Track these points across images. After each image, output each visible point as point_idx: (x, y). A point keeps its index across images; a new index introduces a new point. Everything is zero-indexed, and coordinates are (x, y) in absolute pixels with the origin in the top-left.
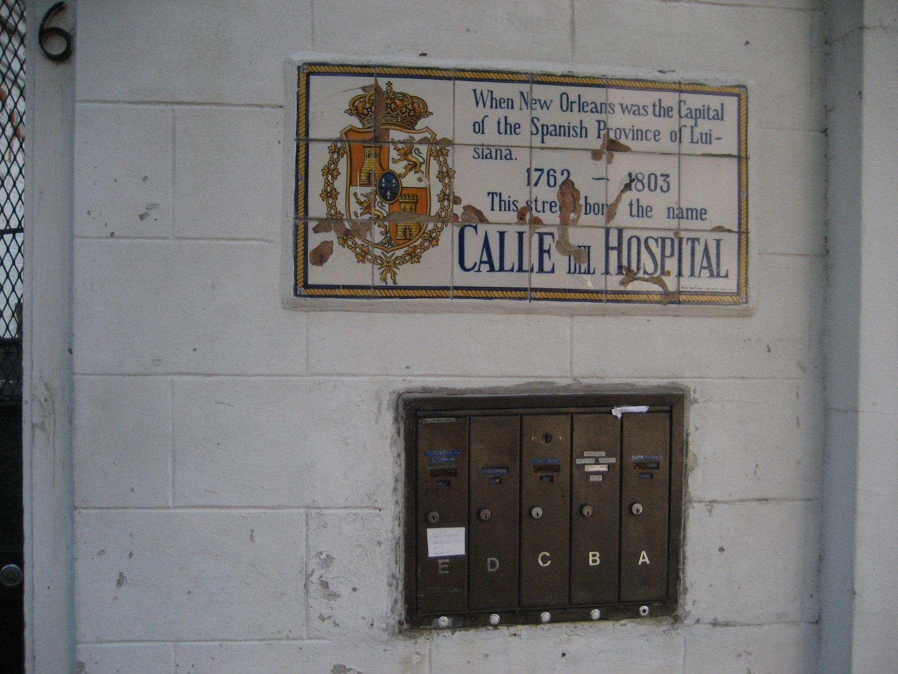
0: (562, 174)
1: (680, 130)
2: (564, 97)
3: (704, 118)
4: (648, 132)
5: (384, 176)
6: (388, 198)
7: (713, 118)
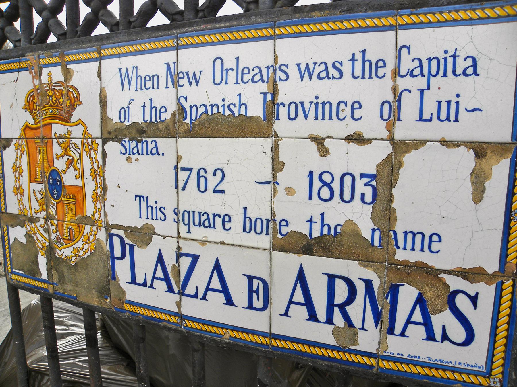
0: (215, 175)
1: (399, 100)
2: (218, 62)
3: (445, 75)
4: (342, 106)
5: (50, 174)
6: (55, 196)
7: (465, 73)
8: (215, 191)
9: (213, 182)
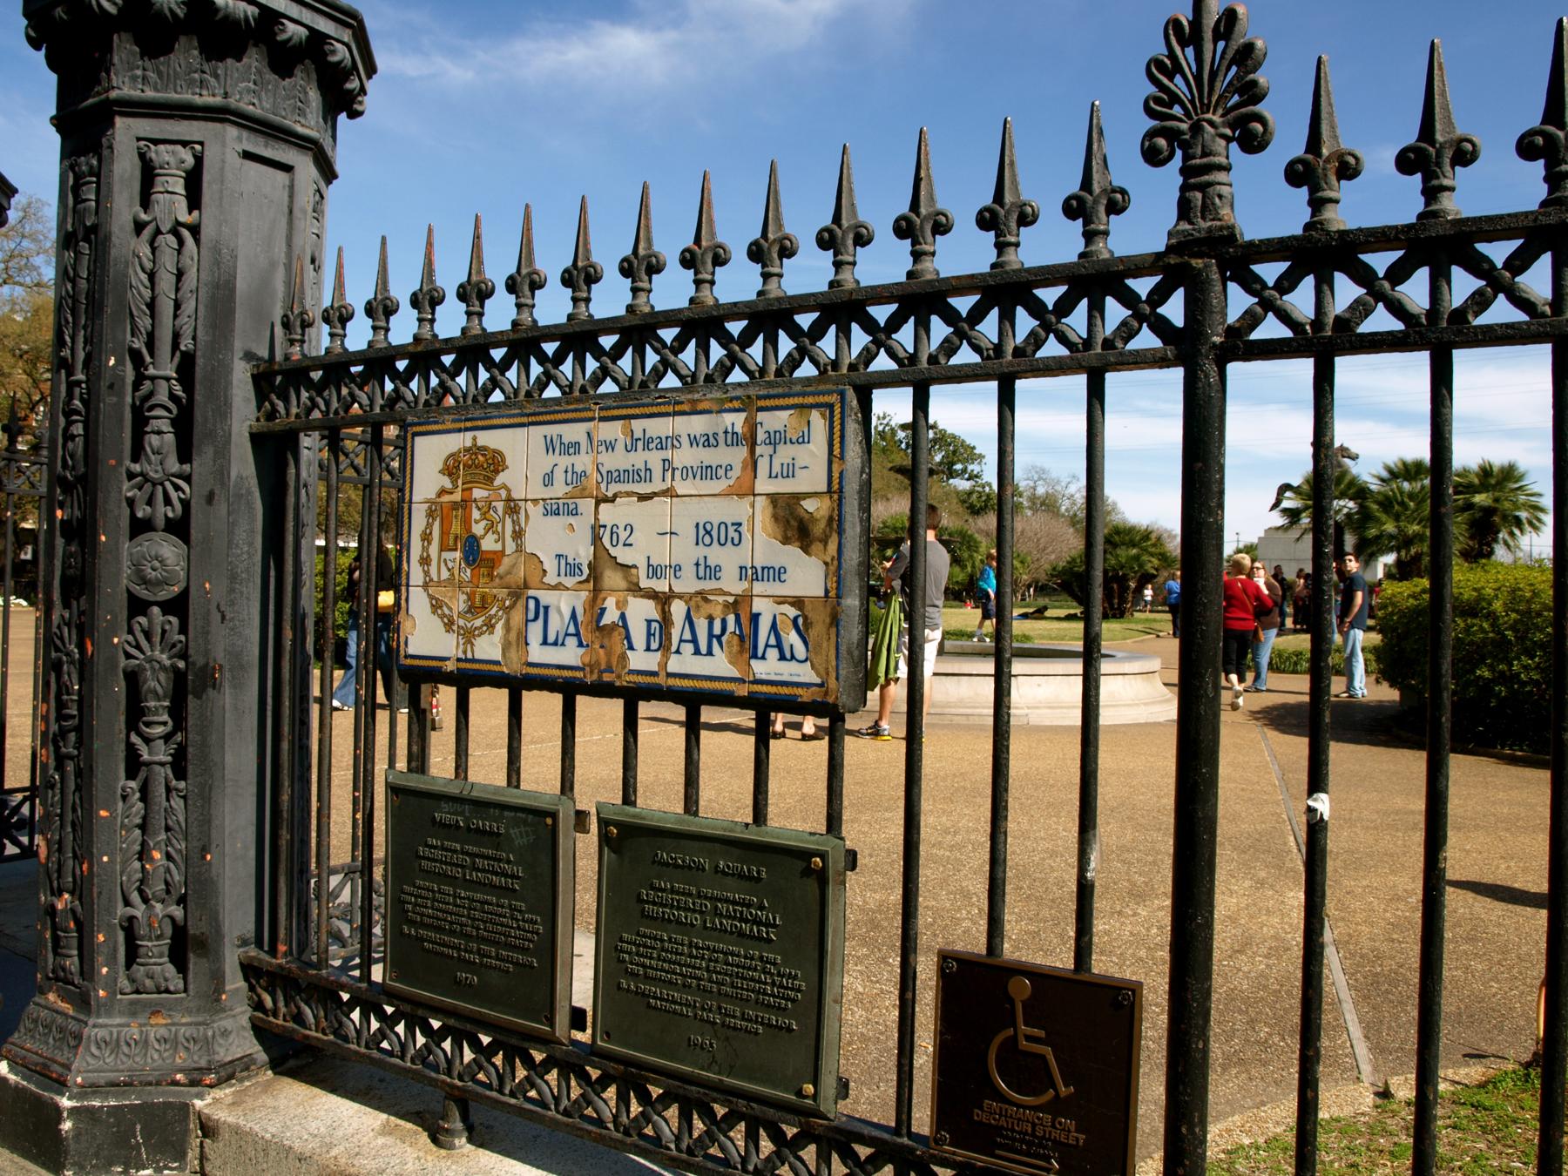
8: (625, 545)
9: (623, 535)
